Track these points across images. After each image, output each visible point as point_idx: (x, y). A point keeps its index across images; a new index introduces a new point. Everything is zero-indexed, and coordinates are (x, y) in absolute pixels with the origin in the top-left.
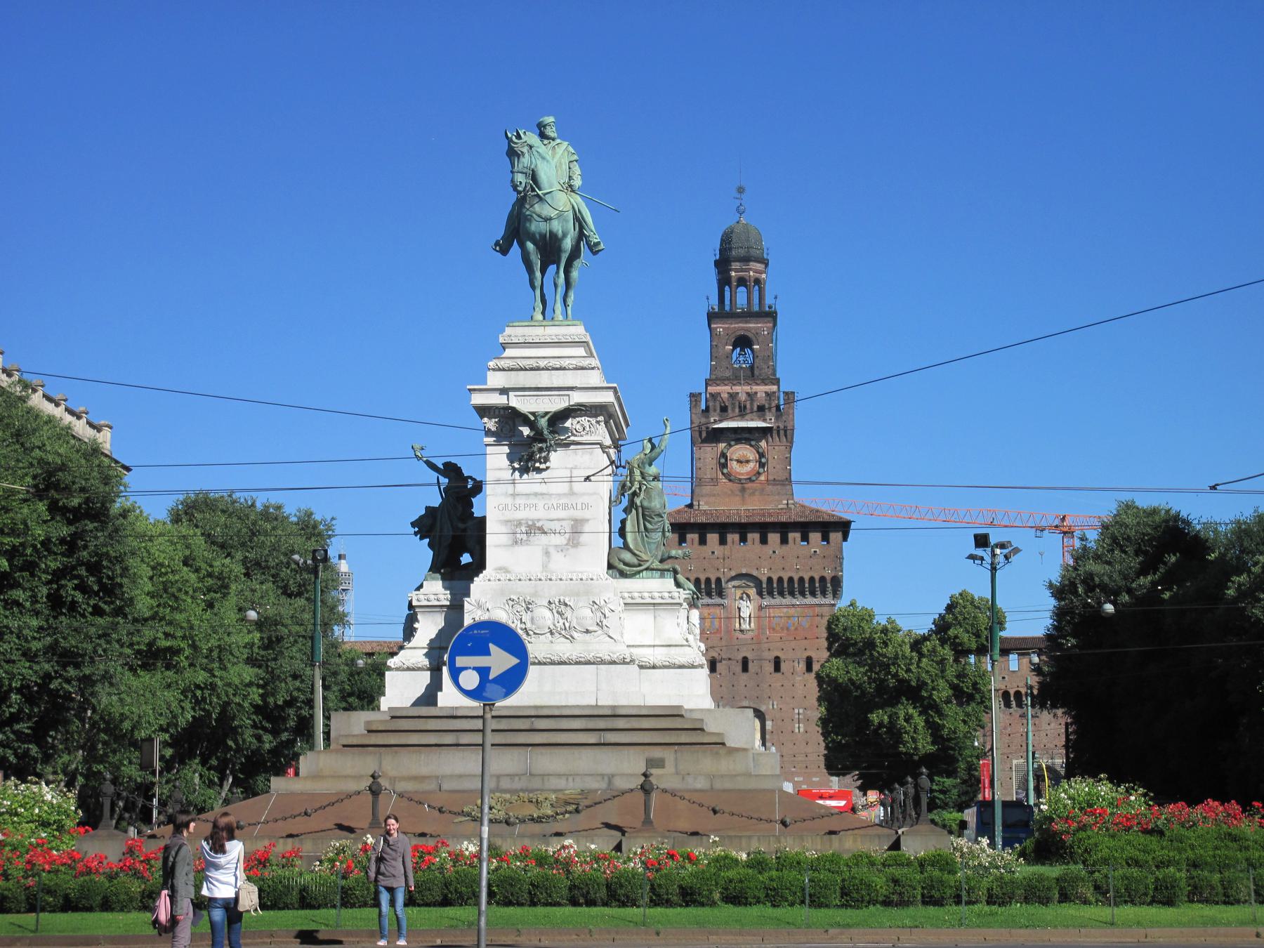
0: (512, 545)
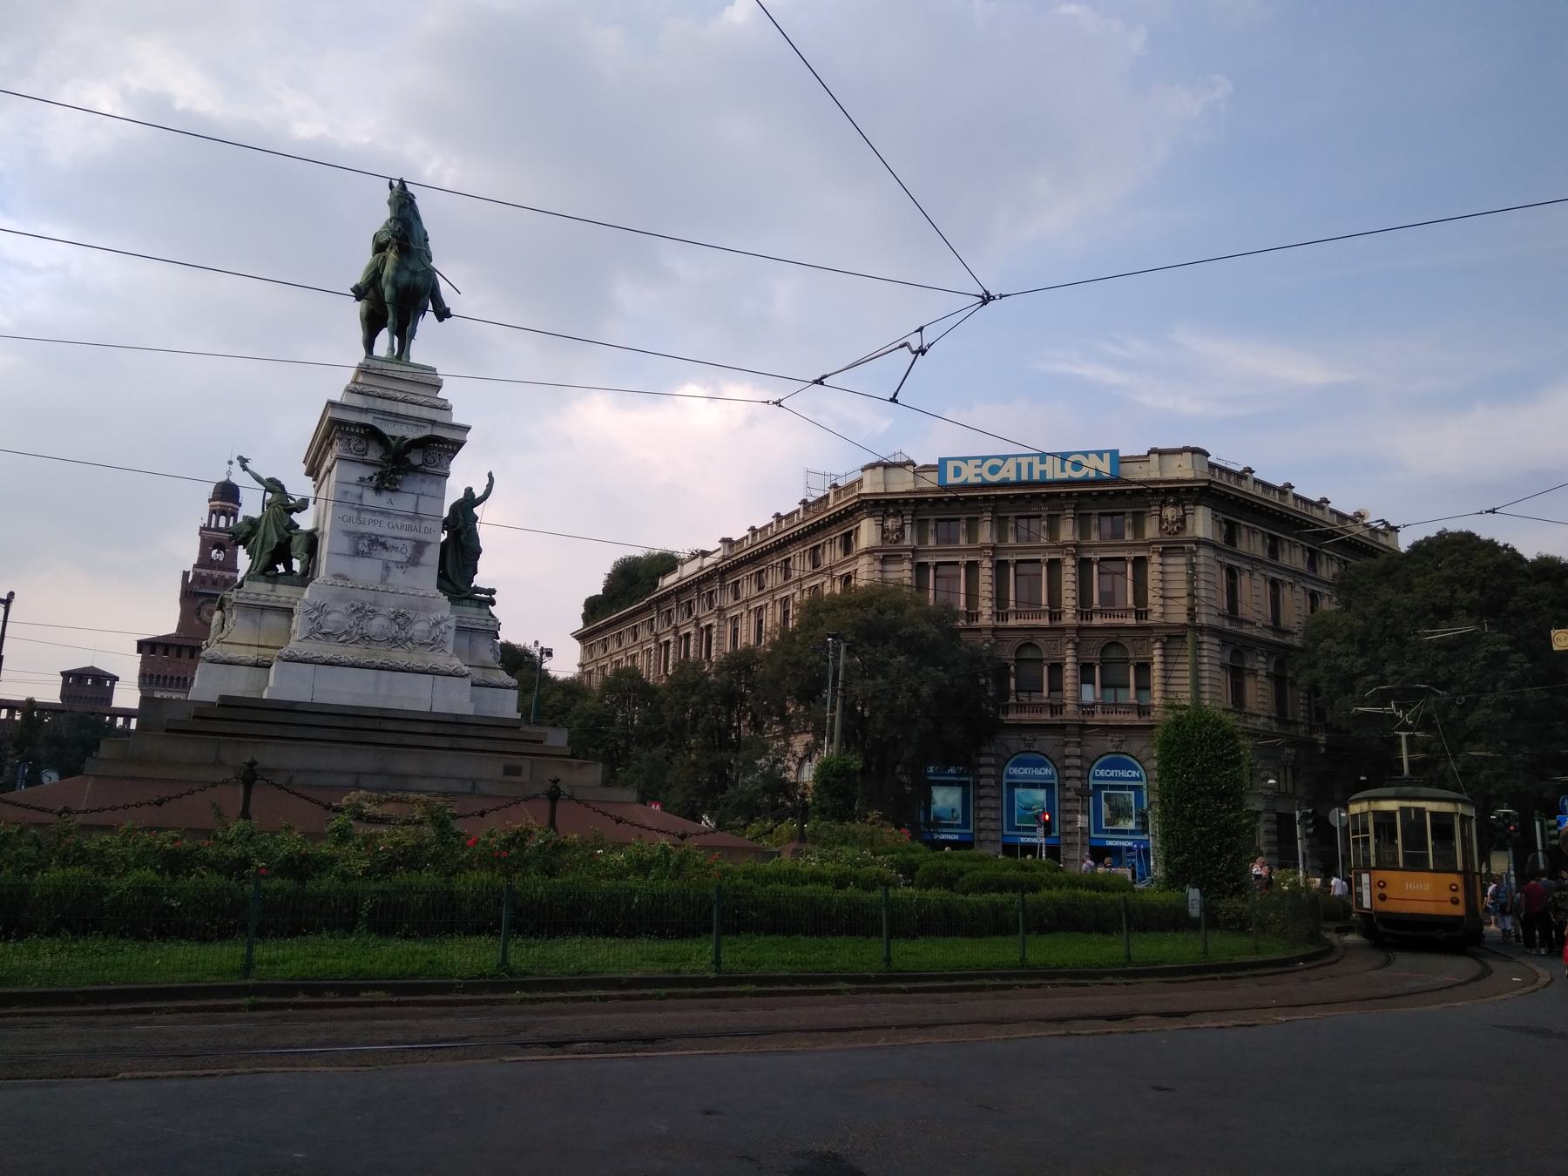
0: (353, 556)
